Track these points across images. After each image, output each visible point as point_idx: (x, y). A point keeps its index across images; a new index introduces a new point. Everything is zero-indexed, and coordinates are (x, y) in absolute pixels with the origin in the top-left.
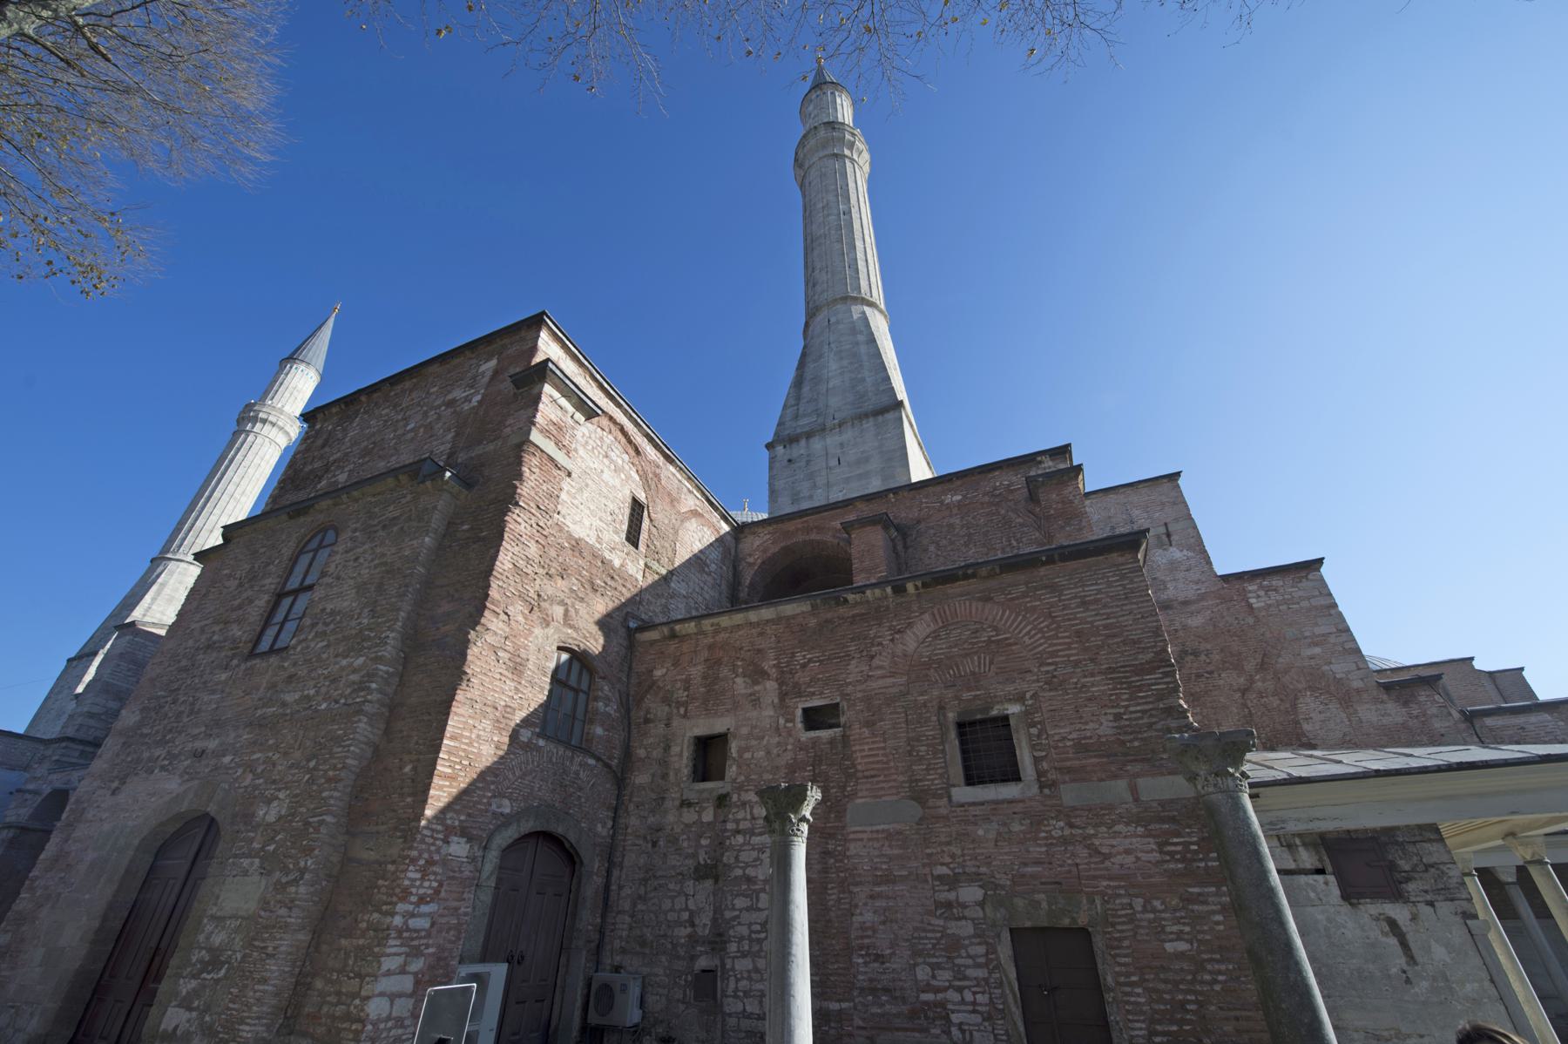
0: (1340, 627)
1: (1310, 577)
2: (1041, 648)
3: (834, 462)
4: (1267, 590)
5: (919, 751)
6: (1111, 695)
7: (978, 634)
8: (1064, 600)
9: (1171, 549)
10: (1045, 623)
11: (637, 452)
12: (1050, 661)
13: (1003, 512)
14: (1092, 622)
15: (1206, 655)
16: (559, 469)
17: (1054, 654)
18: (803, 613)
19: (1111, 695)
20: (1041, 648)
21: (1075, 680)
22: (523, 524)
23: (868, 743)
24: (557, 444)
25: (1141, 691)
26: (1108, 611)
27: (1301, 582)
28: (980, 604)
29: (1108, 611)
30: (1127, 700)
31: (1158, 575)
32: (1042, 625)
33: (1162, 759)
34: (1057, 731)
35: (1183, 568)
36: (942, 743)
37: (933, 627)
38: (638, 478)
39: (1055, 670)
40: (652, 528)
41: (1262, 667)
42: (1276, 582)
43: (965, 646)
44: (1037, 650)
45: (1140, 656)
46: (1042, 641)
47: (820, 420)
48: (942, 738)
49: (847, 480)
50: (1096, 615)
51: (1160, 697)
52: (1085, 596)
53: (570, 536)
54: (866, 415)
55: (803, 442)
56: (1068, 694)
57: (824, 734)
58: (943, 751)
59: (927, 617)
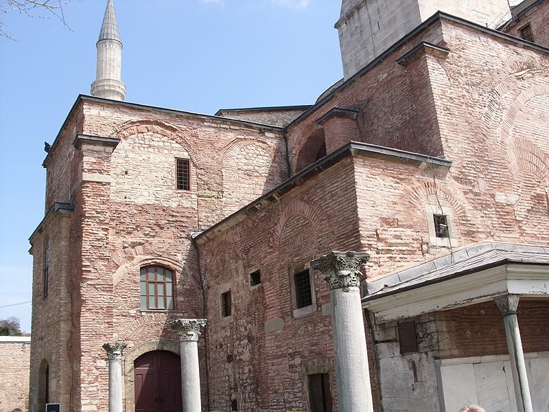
3: (376, 28)
11: (174, 130)
16: (105, 185)
22: (92, 224)
24: (101, 173)
38: (179, 146)
40: (199, 171)
53: (136, 205)
55: (356, 16)
57: (256, 287)
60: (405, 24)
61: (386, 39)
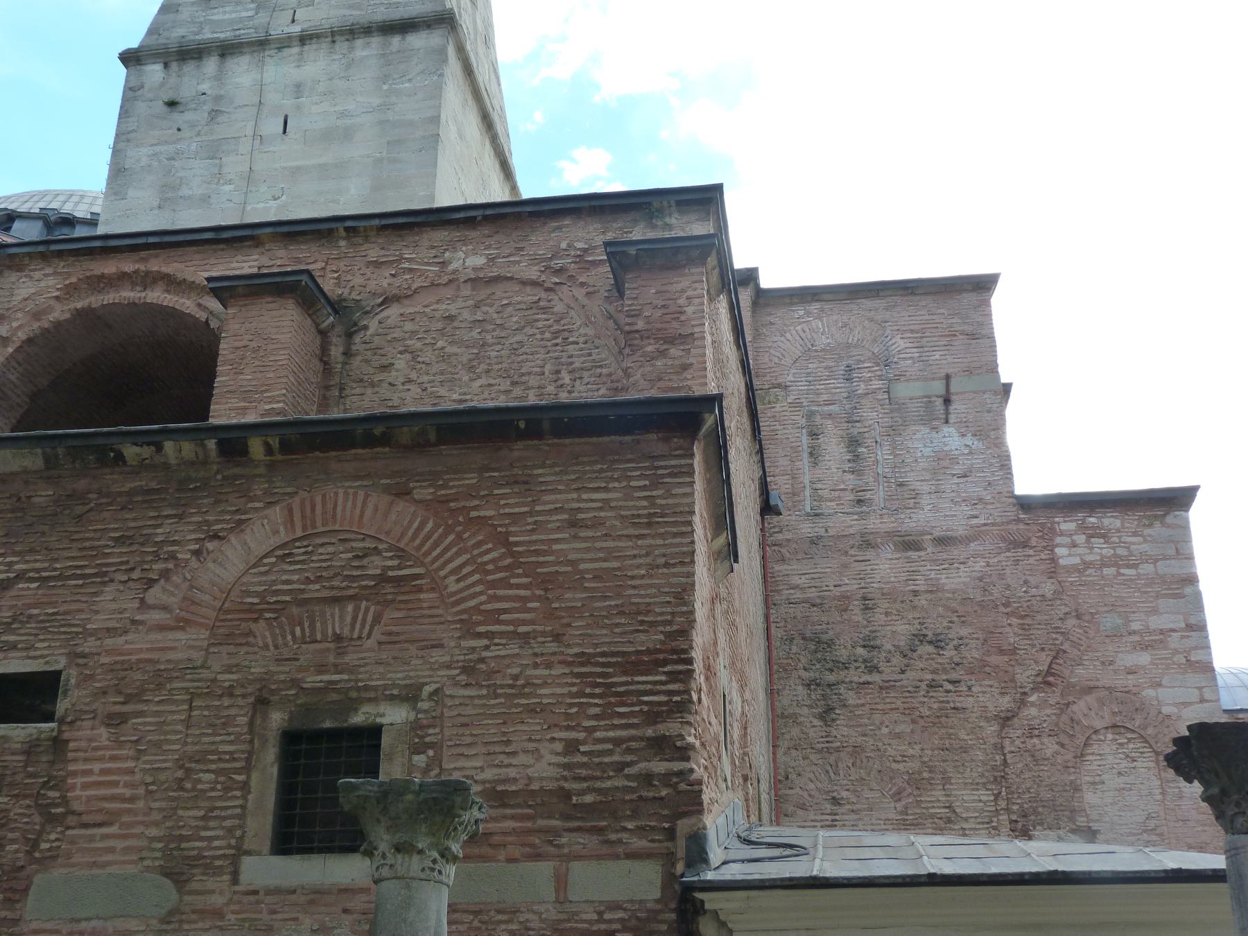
0: (1192, 620)
1: (1169, 519)
2: (472, 603)
4: (1093, 533)
5: (199, 781)
6: (571, 705)
7: (365, 562)
8: (539, 513)
9: (946, 430)
10: (494, 555)
12: (482, 629)
13: (559, 308)
14: (573, 563)
15: (956, 648)
17: (494, 616)
18: (25, 471)
19: (571, 705)
20: (472, 603)
21: (516, 671)
23: (101, 759)
25: (623, 704)
26: (610, 544)
27: (1150, 525)
28: (386, 498)
29: (610, 544)
30: (596, 717)
31: (911, 477)
32: (486, 558)
33: (625, 829)
34: (459, 764)
35: (958, 469)
36: (247, 769)
37: (283, 536)
39: (487, 647)
41: (1046, 680)
42: (1111, 521)
43: (335, 583)
44: (463, 606)
45: (643, 637)
46: (478, 589)
47: (262, 18)
48: (248, 760)
49: (296, 172)
50: (588, 550)
51: (653, 716)
52: (579, 510)
54: (367, 30)
56: (497, 696)
58: (245, 786)
59: (277, 513)
60: (380, 160)
61: (298, 168)
